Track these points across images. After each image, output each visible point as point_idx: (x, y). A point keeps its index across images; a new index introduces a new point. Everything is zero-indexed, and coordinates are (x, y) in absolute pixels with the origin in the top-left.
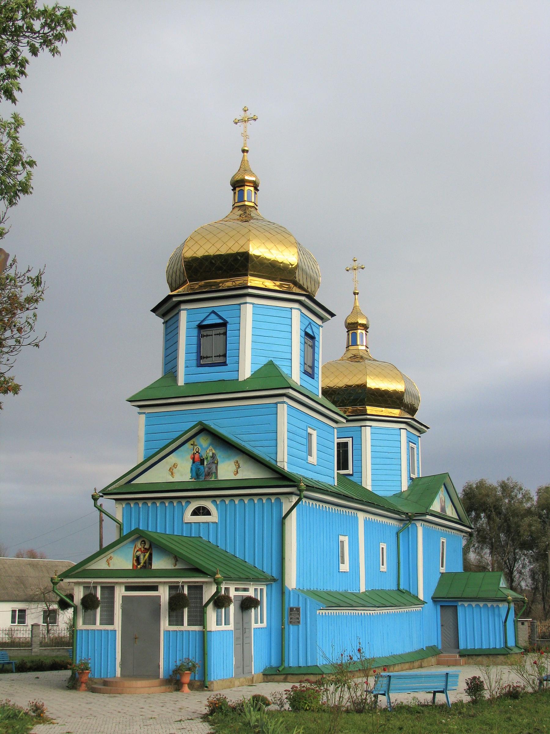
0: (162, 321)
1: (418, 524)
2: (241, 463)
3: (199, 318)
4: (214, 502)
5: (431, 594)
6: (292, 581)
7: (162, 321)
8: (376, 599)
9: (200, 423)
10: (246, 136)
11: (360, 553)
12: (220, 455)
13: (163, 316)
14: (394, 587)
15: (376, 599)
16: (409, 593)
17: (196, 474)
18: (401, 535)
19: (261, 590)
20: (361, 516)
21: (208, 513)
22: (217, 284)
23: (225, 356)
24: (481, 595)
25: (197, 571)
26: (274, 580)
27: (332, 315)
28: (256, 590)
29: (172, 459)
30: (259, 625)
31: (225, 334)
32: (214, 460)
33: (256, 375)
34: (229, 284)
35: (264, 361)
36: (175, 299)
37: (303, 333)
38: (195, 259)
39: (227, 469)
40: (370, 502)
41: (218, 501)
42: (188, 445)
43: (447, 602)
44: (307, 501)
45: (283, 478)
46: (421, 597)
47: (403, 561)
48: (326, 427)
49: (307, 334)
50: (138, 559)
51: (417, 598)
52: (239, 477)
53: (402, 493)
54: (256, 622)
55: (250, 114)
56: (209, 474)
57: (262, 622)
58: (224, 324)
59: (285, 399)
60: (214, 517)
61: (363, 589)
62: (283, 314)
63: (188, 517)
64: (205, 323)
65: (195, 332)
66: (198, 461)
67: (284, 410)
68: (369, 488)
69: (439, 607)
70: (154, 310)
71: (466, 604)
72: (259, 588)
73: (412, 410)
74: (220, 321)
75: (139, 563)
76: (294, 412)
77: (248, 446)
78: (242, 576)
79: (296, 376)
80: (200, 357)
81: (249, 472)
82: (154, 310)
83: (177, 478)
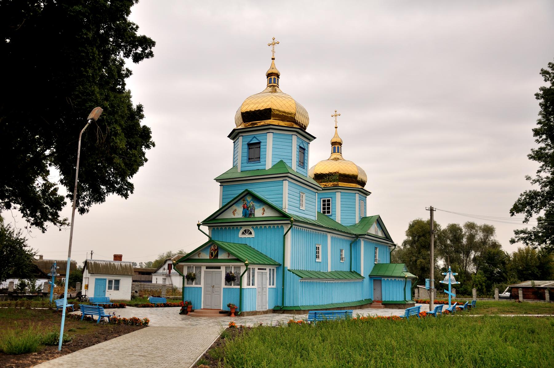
0: (233, 141)
1: (361, 239)
2: (265, 209)
3: (248, 140)
4: (253, 228)
5: (369, 273)
6: (288, 265)
7: (233, 141)
8: (337, 277)
9: (247, 190)
10: (273, 52)
11: (331, 254)
12: (256, 205)
13: (233, 139)
14: (348, 270)
15: (337, 277)
16: (356, 273)
17: (245, 215)
18: (352, 245)
19: (273, 270)
20: (329, 236)
21: (251, 233)
22: (256, 124)
23: (259, 158)
24: (393, 275)
25: (238, 260)
26: (280, 265)
27: (315, 138)
28: (270, 270)
29: (234, 207)
30: (272, 286)
31: (260, 147)
32: (253, 209)
33: (274, 167)
34: (262, 123)
35: (279, 160)
36: (236, 131)
37: (298, 147)
38: (247, 112)
39: (259, 212)
40: (337, 230)
41: (255, 227)
42: (241, 201)
43: (376, 278)
44: (296, 227)
45: (284, 216)
46: (362, 275)
47: (353, 257)
48: (310, 192)
49: (300, 147)
50: (212, 254)
51: (360, 275)
52: (264, 215)
53: (356, 224)
54: (270, 285)
55: (276, 41)
56: (250, 214)
57: (273, 285)
58: (259, 143)
59: (287, 178)
60: (253, 235)
61: (329, 270)
62: (288, 137)
63: (240, 235)
64: (252, 142)
65: (246, 147)
66: (245, 208)
67: (286, 184)
68: (340, 222)
69: (373, 281)
70: (229, 136)
71: (386, 279)
72: (272, 269)
73: (363, 184)
74: (257, 141)
75: (212, 256)
76: (291, 185)
77: (270, 201)
78: (255, 262)
79: (294, 166)
80: (249, 159)
81: (269, 213)
82: (229, 136)
83: (237, 216)
